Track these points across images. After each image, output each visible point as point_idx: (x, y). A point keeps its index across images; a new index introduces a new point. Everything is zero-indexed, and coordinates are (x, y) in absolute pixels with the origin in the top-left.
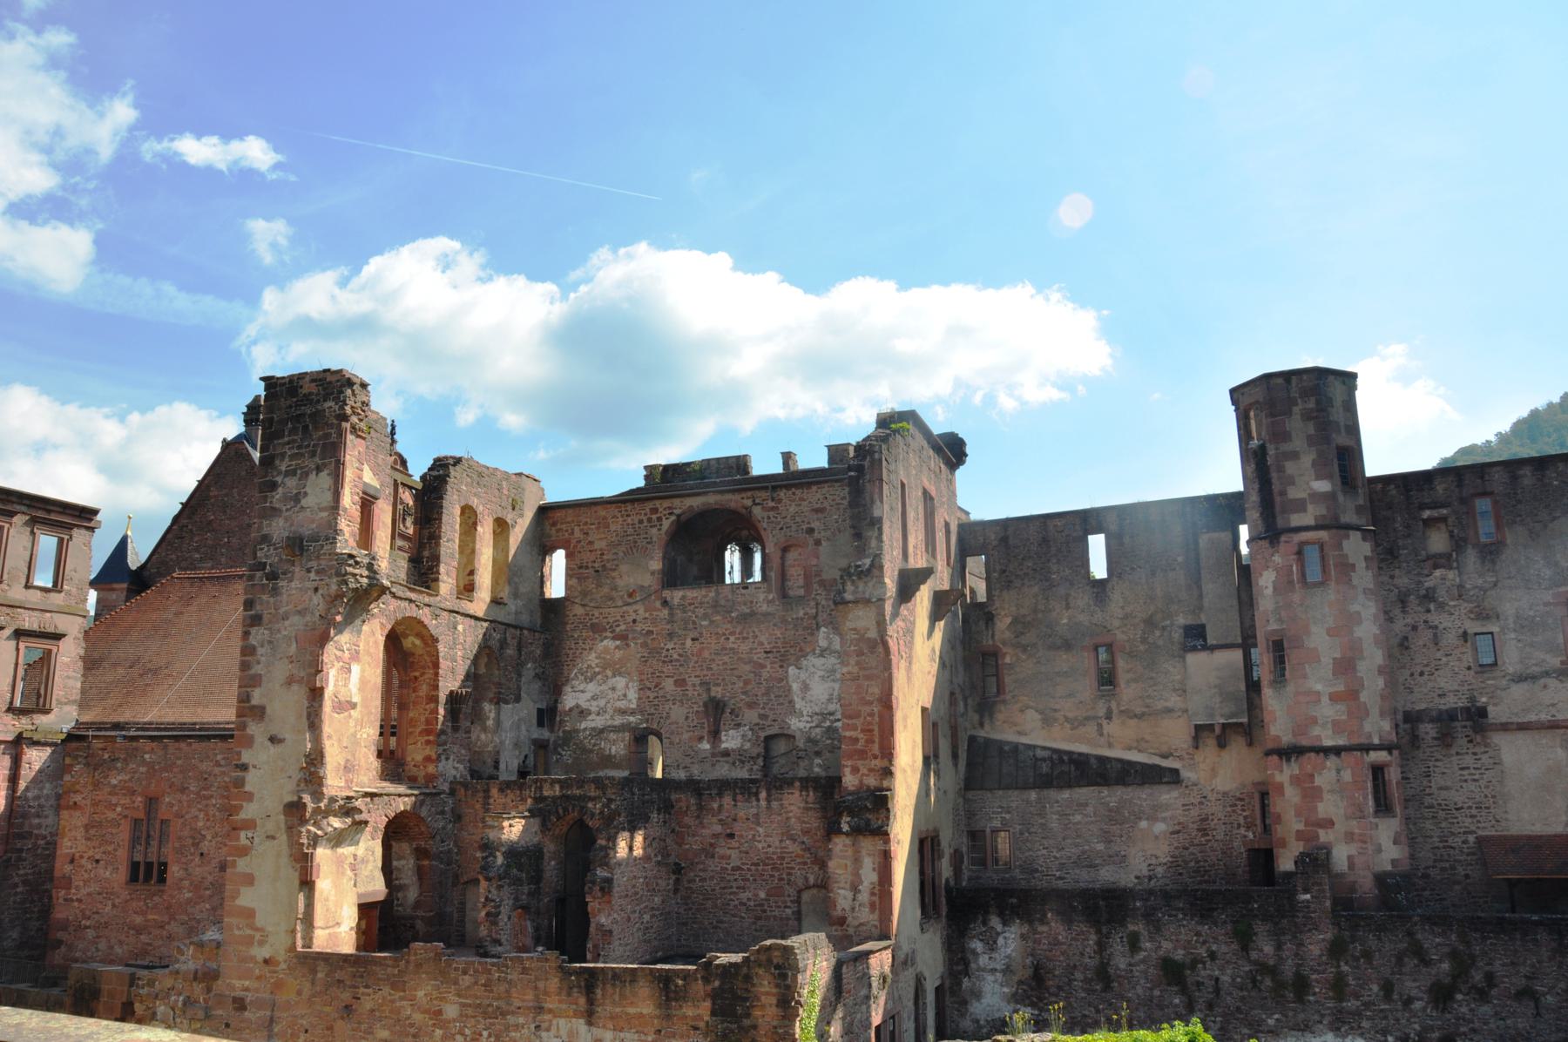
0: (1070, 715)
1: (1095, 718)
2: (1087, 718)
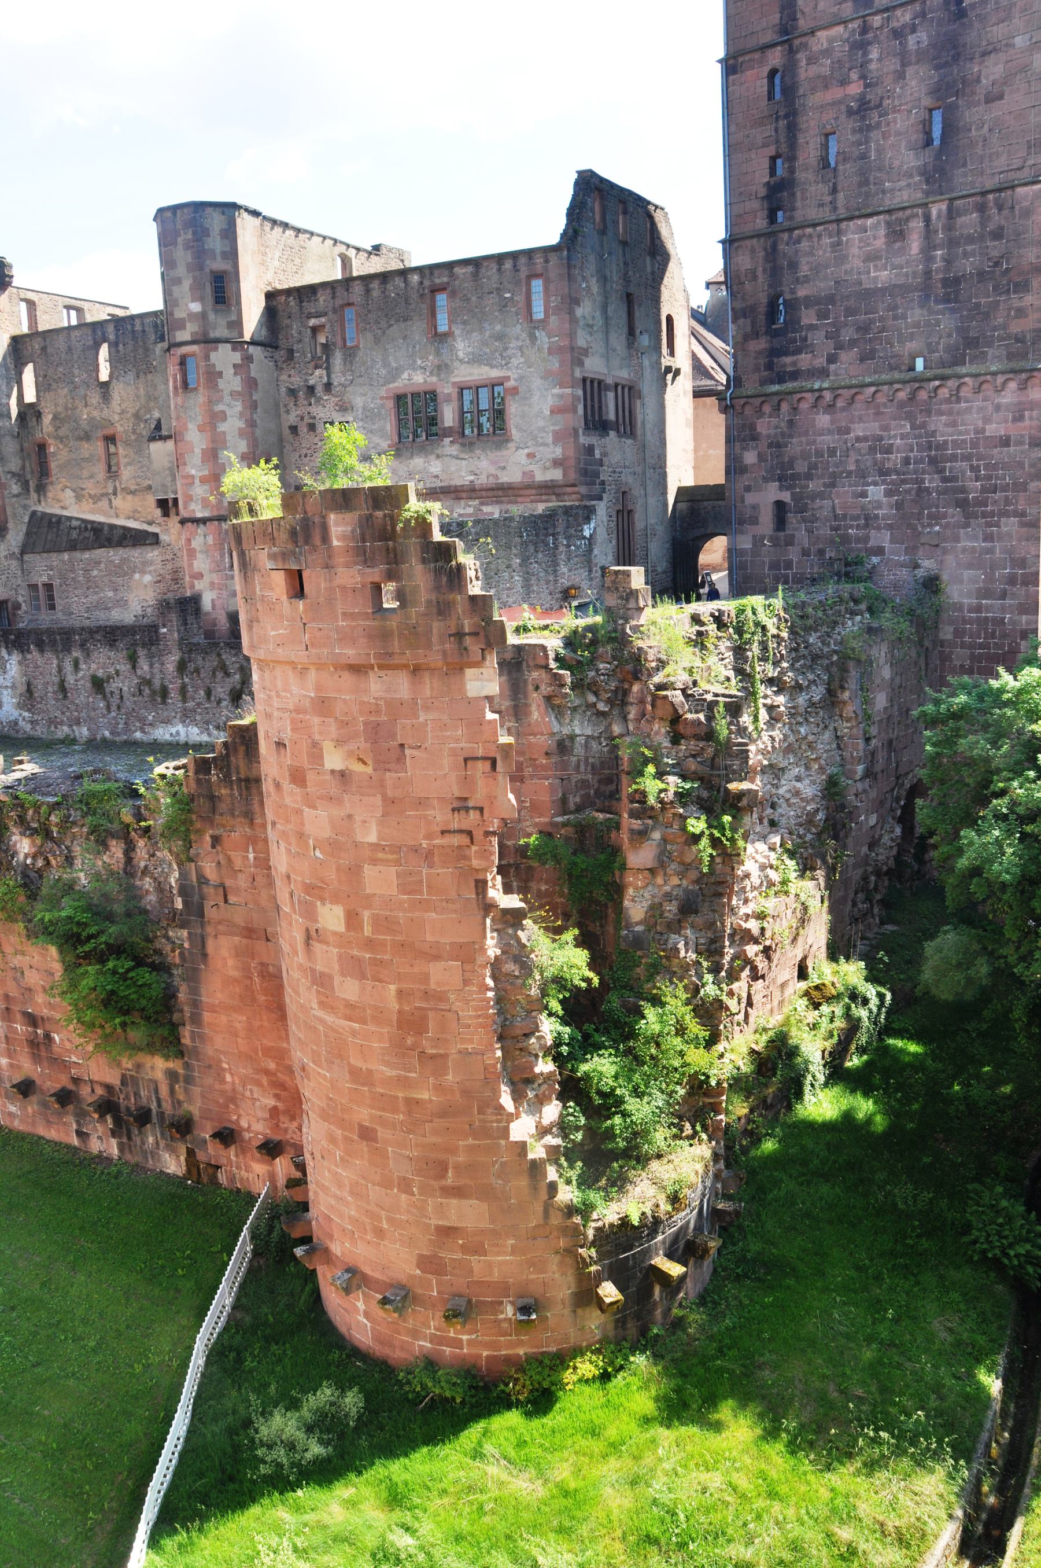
0: (92, 493)
1: (107, 494)
2: (102, 495)
